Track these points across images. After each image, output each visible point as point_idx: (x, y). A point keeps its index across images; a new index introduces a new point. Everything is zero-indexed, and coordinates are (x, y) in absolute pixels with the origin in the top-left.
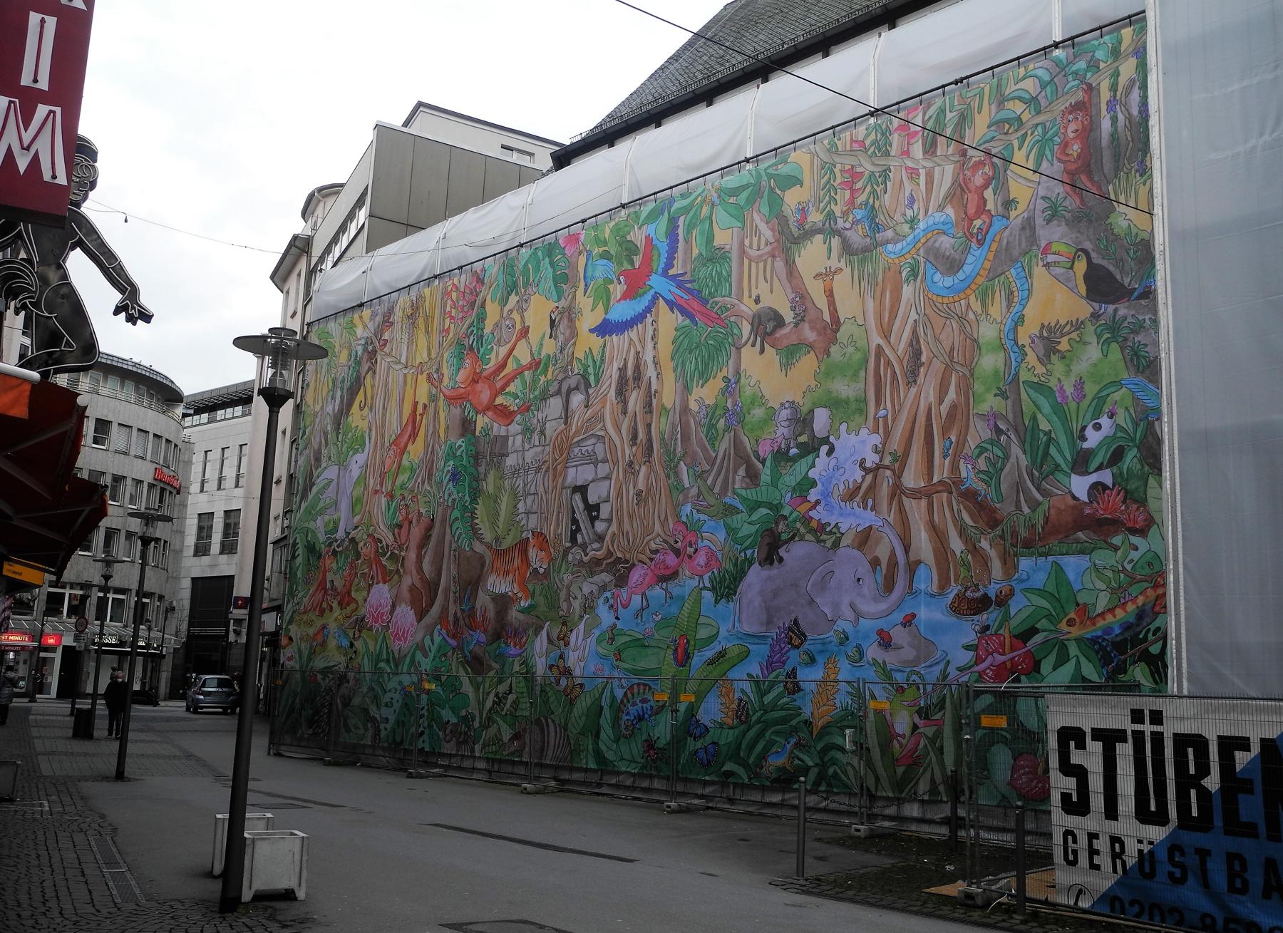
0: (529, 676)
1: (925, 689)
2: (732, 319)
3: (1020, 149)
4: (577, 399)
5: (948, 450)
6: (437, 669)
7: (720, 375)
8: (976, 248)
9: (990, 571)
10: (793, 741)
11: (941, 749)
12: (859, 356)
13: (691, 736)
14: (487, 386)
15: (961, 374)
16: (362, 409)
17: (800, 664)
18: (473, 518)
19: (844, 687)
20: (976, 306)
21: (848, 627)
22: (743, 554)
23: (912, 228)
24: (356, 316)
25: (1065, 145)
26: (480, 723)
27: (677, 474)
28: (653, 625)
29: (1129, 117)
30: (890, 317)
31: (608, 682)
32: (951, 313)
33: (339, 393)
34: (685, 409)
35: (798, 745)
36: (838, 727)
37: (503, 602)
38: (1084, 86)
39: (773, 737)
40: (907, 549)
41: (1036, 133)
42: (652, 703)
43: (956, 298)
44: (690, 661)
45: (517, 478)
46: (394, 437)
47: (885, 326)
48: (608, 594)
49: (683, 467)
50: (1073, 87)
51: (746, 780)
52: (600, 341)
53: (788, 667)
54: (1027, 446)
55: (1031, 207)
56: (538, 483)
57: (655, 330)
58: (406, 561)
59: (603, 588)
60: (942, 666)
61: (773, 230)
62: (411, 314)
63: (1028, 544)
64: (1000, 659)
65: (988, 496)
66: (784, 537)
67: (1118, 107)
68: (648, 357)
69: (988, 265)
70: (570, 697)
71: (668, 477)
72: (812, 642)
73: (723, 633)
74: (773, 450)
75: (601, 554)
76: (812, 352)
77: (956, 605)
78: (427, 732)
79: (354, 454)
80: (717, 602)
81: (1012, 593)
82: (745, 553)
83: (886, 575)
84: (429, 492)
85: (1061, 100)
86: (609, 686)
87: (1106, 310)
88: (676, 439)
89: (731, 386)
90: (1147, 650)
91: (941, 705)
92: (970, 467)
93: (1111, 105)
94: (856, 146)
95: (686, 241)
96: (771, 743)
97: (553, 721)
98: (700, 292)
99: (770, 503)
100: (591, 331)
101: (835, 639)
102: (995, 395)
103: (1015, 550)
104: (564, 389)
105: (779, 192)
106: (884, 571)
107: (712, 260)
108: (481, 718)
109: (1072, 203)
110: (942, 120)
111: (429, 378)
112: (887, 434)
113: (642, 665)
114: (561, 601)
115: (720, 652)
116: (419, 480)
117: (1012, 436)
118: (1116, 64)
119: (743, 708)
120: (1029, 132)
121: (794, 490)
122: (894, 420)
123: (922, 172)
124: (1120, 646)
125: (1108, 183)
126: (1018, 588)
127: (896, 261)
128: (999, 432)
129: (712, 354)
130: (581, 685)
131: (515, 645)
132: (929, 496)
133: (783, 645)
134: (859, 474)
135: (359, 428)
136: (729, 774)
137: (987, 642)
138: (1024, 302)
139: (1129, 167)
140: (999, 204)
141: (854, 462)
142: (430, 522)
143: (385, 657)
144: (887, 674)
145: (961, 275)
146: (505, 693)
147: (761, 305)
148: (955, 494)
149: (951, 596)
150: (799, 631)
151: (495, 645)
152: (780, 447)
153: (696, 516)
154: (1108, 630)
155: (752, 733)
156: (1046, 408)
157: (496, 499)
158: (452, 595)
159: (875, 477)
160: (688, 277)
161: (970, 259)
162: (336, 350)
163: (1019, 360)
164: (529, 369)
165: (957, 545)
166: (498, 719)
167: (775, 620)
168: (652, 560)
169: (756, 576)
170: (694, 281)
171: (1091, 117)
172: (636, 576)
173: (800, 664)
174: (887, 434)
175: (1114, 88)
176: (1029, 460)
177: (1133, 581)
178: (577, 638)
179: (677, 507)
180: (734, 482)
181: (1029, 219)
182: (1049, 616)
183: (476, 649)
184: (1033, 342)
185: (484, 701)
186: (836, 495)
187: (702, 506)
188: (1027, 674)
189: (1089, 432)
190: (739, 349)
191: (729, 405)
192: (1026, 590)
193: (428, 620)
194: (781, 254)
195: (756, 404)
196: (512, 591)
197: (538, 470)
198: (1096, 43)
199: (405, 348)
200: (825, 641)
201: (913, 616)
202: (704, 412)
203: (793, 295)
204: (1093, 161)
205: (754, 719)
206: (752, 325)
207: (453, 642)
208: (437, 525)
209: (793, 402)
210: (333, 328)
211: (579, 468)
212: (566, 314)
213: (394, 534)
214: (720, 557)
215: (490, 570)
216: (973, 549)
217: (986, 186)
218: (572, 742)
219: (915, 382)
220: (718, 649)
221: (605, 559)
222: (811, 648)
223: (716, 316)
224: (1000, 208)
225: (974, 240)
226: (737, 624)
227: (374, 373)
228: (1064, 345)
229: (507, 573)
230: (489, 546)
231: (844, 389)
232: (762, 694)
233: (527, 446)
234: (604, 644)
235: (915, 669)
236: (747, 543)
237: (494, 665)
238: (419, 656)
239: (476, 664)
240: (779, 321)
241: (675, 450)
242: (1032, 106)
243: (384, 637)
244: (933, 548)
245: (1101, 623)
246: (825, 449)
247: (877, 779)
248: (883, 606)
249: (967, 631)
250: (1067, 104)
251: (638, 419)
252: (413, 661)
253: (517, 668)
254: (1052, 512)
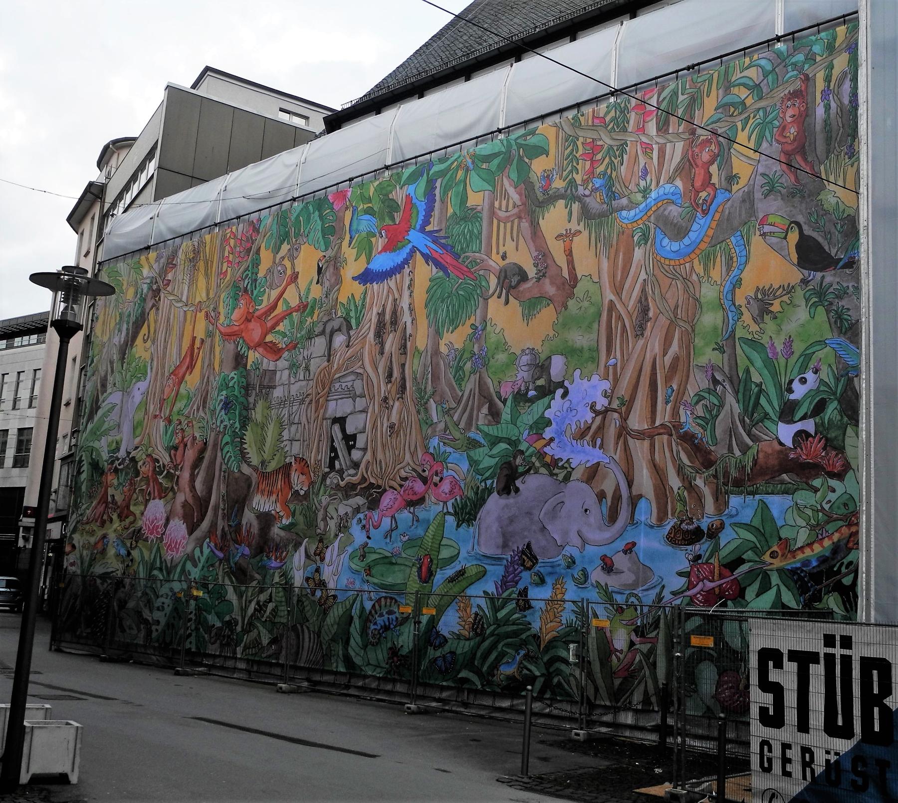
0: (287, 587)
1: (642, 610)
2: (481, 272)
3: (743, 130)
4: (339, 340)
5: (670, 397)
6: (205, 578)
7: (468, 323)
8: (701, 217)
9: (703, 507)
10: (522, 653)
11: (654, 665)
12: (592, 310)
13: (431, 646)
14: (258, 324)
15: (684, 329)
16: (145, 341)
17: (531, 584)
18: (242, 443)
19: (569, 606)
20: (699, 269)
21: (576, 553)
22: (483, 484)
23: (645, 197)
24: (143, 258)
25: (783, 128)
26: (242, 627)
27: (426, 410)
28: (400, 544)
29: (841, 106)
30: (622, 276)
31: (358, 595)
32: (677, 274)
33: (125, 326)
34: (436, 352)
35: (527, 657)
36: (564, 642)
37: (266, 520)
38: (802, 77)
39: (504, 649)
40: (630, 484)
41: (758, 117)
42: (397, 615)
43: (682, 261)
44: (432, 578)
45: (283, 408)
46: (173, 368)
47: (617, 284)
48: (361, 516)
49: (432, 404)
50: (791, 77)
51: (479, 687)
52: (362, 288)
53: (521, 586)
54: (740, 396)
55: (751, 182)
56: (301, 413)
57: (411, 280)
58: (180, 480)
59: (357, 510)
60: (657, 590)
61: (520, 194)
62: (193, 258)
63: (738, 484)
64: (710, 585)
65: (704, 439)
66: (521, 470)
67: (831, 96)
68: (405, 303)
69: (711, 233)
70: (324, 607)
71: (418, 412)
72: (542, 565)
73: (463, 554)
74: (514, 392)
75: (355, 479)
76: (551, 305)
77: (672, 536)
78: (194, 634)
79: (137, 382)
80: (458, 526)
81: (722, 526)
82: (486, 483)
83: (610, 507)
84: (203, 419)
85: (781, 87)
86: (359, 599)
87: (814, 277)
88: (427, 379)
89: (478, 333)
90: (840, 581)
91: (656, 624)
92: (689, 413)
93: (825, 94)
94: (597, 122)
95: (442, 201)
96: (503, 654)
97: (308, 628)
98: (453, 247)
99: (509, 439)
100: (354, 278)
101: (563, 563)
102: (713, 349)
103: (726, 488)
104: (328, 330)
105: (527, 160)
106: (609, 503)
107: (464, 219)
108: (243, 623)
109: (788, 180)
110: (674, 102)
111: (207, 315)
112: (616, 381)
113: (390, 580)
114: (319, 520)
115: (460, 571)
116: (195, 407)
117: (727, 387)
118: (830, 58)
119: (479, 622)
120: (752, 116)
121: (531, 427)
122: (622, 369)
123: (655, 147)
124: (816, 577)
125: (820, 163)
126: (727, 523)
127: (630, 226)
128: (715, 382)
129: (462, 305)
130: (335, 597)
131: (276, 559)
132: (652, 437)
133: (516, 567)
134: (589, 416)
135: (142, 359)
136: (465, 680)
137: (698, 570)
138: (742, 267)
139: (839, 150)
140: (723, 179)
141: (586, 405)
142: (203, 445)
143: (158, 564)
144: (608, 595)
145: (686, 241)
146: (265, 601)
147: (507, 261)
148: (674, 437)
149: (668, 528)
150: (531, 554)
151: (258, 558)
152: (520, 389)
153: (443, 448)
154: (806, 563)
155: (486, 644)
156: (759, 363)
157: (263, 427)
158: (220, 512)
159: (604, 418)
160: (442, 234)
161: (695, 227)
162: (124, 288)
163: (736, 318)
164: (297, 311)
165: (675, 482)
166: (258, 625)
167: (510, 544)
168: (401, 486)
169: (494, 504)
170: (448, 237)
171: (807, 104)
172: (387, 500)
173: (531, 584)
174: (616, 381)
175: (828, 79)
176: (742, 408)
177: (830, 519)
178: (332, 554)
179: (426, 439)
180: (477, 419)
181: (749, 193)
182: (754, 549)
183: (241, 561)
184: (749, 303)
185: (247, 607)
186: (568, 433)
187: (448, 439)
188: (733, 600)
189: (796, 385)
190: (486, 300)
191: (476, 350)
192: (735, 524)
193: (198, 533)
194: (527, 216)
195: (500, 349)
196: (275, 510)
197: (302, 402)
198: (813, 38)
199: (186, 288)
200: (555, 564)
201: (634, 544)
202: (453, 355)
203: (536, 254)
204: (807, 144)
205: (488, 632)
206: (499, 278)
207: (221, 555)
208: (210, 448)
209: (533, 349)
210: (122, 268)
211: (339, 401)
212: (332, 263)
213: (170, 456)
214: (462, 486)
215: (255, 491)
216: (690, 486)
217: (711, 162)
218: (324, 647)
219: (642, 335)
220: (458, 568)
221: (359, 484)
222: (542, 570)
223: (466, 269)
224: (724, 183)
225: (699, 210)
226: (476, 547)
227: (158, 309)
228: (776, 307)
229: (270, 493)
230: (255, 469)
231: (579, 339)
232: (496, 610)
233: (292, 380)
234: (356, 560)
235: (634, 591)
236: (487, 474)
237: (257, 576)
238: (189, 566)
239: (240, 574)
240: (523, 276)
241: (425, 388)
242: (755, 92)
243: (158, 549)
244: (654, 484)
245: (800, 556)
246: (560, 392)
247: (597, 689)
248: (607, 534)
249: (681, 559)
250: (787, 92)
251: (394, 359)
252: (183, 570)
253: (277, 579)
254: (761, 455)
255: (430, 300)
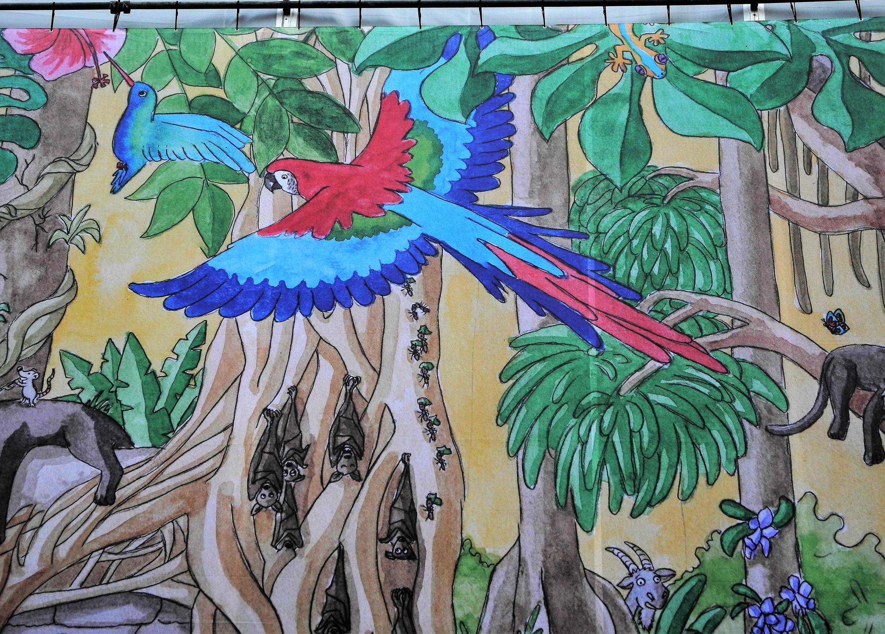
129: (668, 435)
170: (586, 236)
255: (521, 402)
